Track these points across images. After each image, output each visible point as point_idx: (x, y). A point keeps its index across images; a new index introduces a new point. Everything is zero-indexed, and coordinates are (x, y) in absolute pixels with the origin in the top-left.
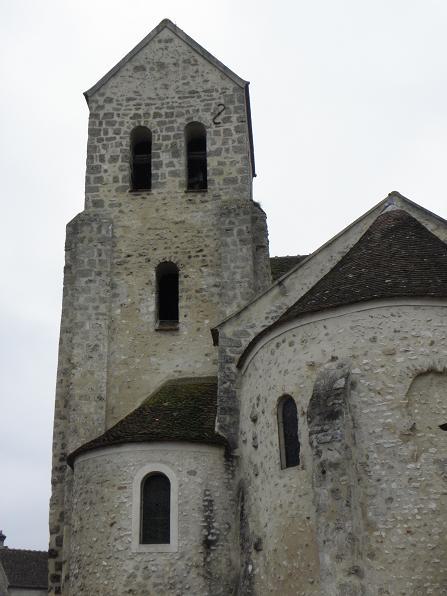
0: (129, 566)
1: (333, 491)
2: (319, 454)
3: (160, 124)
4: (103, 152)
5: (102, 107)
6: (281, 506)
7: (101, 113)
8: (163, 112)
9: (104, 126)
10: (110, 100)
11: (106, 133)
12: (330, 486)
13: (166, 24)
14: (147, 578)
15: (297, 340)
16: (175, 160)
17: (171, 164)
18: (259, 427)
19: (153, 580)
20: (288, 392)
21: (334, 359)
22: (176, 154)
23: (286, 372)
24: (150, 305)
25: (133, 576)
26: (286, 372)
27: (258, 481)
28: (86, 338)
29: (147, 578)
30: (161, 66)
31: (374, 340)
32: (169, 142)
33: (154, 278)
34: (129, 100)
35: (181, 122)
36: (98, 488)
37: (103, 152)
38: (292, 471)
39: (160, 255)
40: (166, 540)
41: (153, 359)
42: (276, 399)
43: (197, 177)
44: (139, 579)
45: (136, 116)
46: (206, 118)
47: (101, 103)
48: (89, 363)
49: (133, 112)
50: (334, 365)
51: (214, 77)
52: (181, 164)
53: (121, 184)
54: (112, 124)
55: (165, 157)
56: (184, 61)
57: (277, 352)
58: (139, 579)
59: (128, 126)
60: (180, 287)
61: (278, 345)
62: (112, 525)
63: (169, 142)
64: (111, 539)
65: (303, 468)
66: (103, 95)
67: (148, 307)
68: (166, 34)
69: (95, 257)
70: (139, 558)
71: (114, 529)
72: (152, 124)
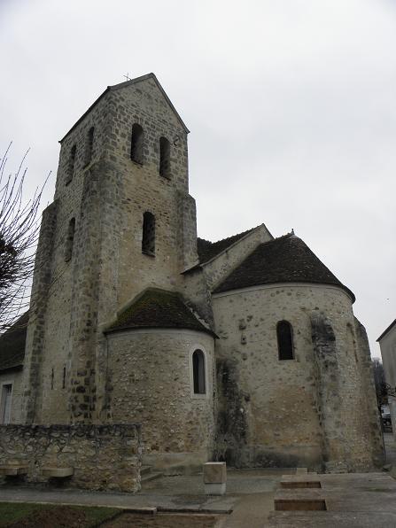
0: (188, 407)
1: (332, 376)
2: (323, 357)
3: (148, 128)
4: (117, 128)
5: (119, 101)
6: (280, 379)
7: (118, 104)
8: (150, 123)
9: (119, 113)
10: (123, 100)
11: (120, 117)
12: (330, 374)
13: (152, 76)
14: (198, 414)
15: (294, 293)
16: (156, 155)
17: (153, 155)
18: (246, 333)
19: (201, 416)
20: (287, 318)
21: (317, 309)
22: (156, 150)
23: (285, 308)
24: (139, 237)
25: (191, 413)
26: (285, 308)
27: (247, 363)
28: (108, 245)
29: (198, 414)
30: (150, 97)
31: (333, 304)
32: (153, 142)
33: (142, 220)
34: (133, 105)
35: (158, 133)
36: (163, 354)
37: (117, 128)
38: (287, 363)
39: (146, 207)
40: (204, 393)
41: (140, 271)
42: (276, 322)
43: (164, 170)
44: (195, 415)
45: (135, 117)
46: (171, 139)
47: (118, 98)
48: (110, 262)
49: (134, 114)
50: (317, 312)
51: (174, 120)
52: (157, 157)
53: (126, 153)
54: (124, 115)
55: (151, 150)
56: (161, 102)
57: (277, 296)
58: (195, 415)
59: (131, 121)
60: (156, 231)
61: (278, 292)
62: (175, 380)
63: (153, 142)
64: (176, 389)
65: (298, 361)
66: (119, 94)
67: (139, 236)
68: (152, 81)
69: (115, 192)
70: (194, 402)
71: (177, 382)
72: (145, 126)
